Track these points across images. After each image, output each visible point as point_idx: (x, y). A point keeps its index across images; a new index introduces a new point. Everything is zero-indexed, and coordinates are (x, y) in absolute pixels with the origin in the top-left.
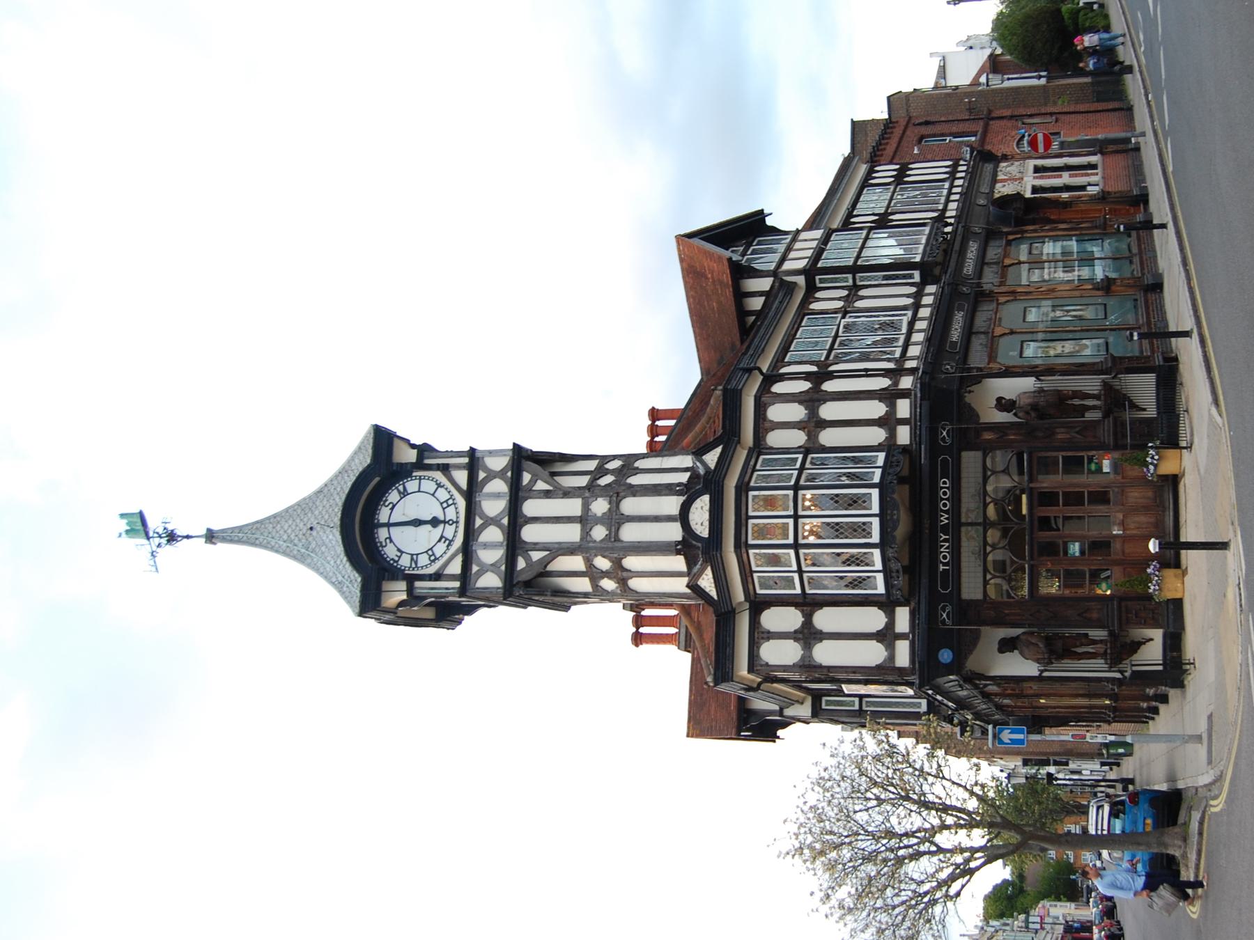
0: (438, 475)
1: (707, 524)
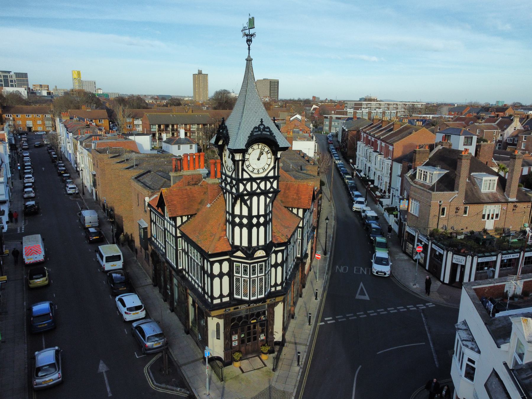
0: (272, 165)
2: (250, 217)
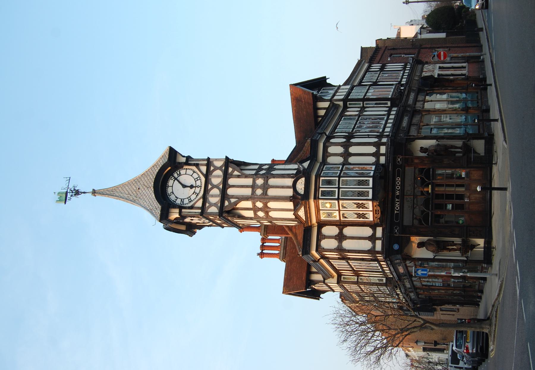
0: (194, 168)
1: (303, 189)
2: (252, 198)
